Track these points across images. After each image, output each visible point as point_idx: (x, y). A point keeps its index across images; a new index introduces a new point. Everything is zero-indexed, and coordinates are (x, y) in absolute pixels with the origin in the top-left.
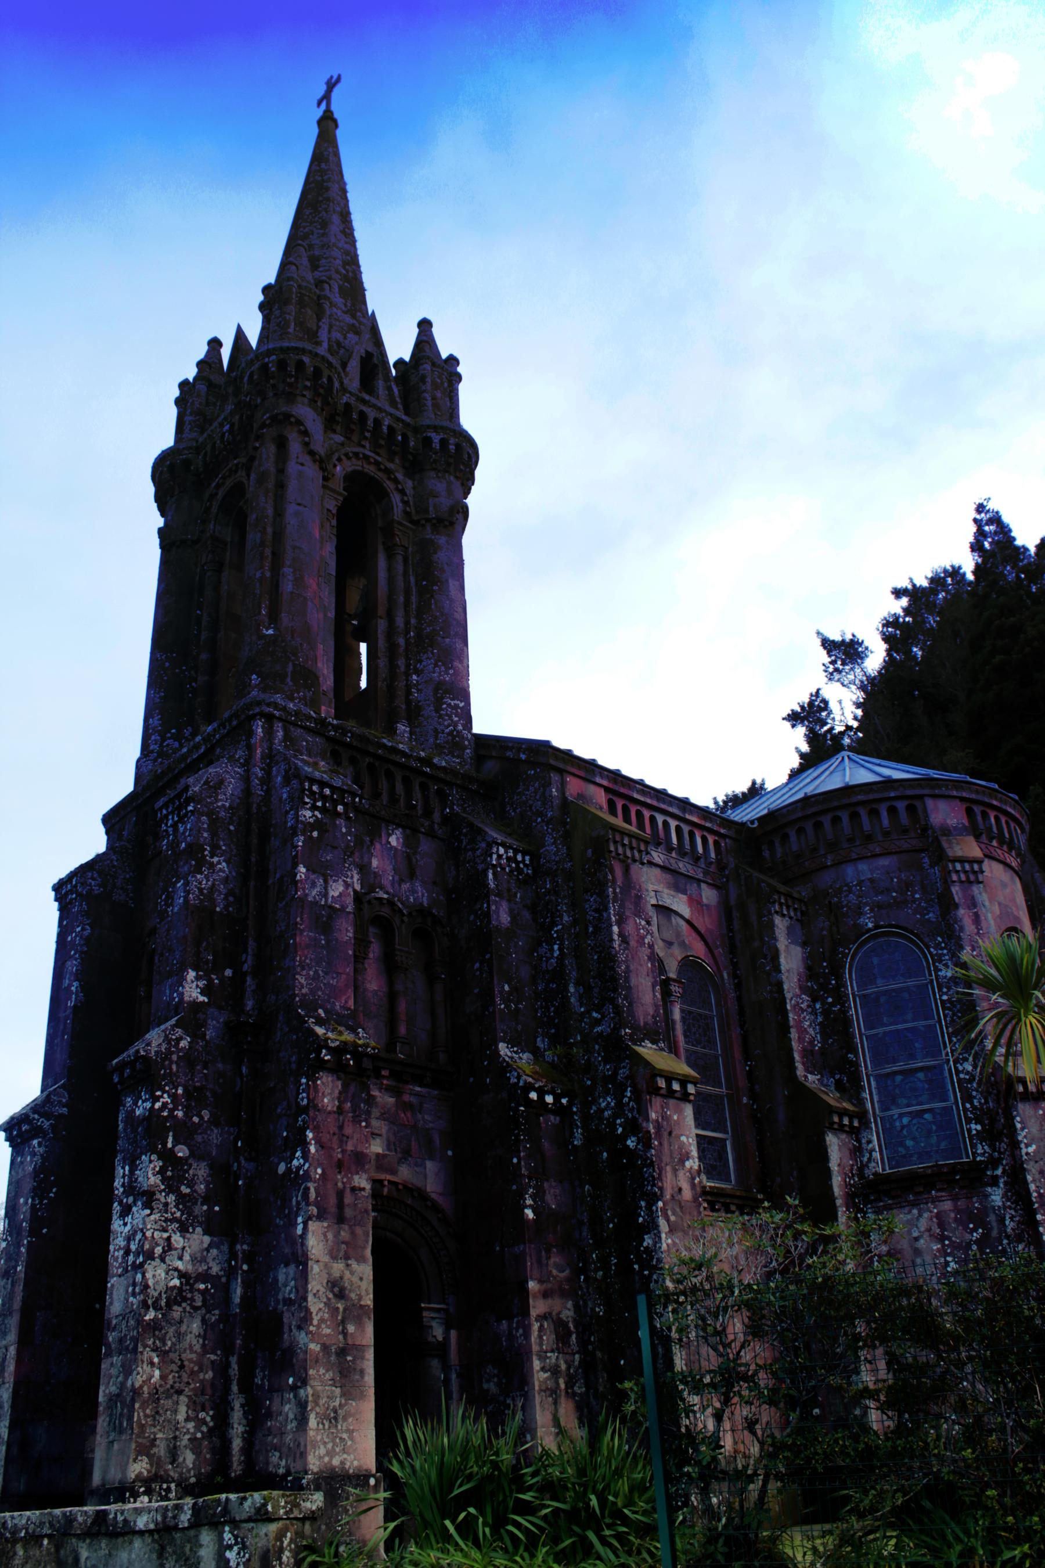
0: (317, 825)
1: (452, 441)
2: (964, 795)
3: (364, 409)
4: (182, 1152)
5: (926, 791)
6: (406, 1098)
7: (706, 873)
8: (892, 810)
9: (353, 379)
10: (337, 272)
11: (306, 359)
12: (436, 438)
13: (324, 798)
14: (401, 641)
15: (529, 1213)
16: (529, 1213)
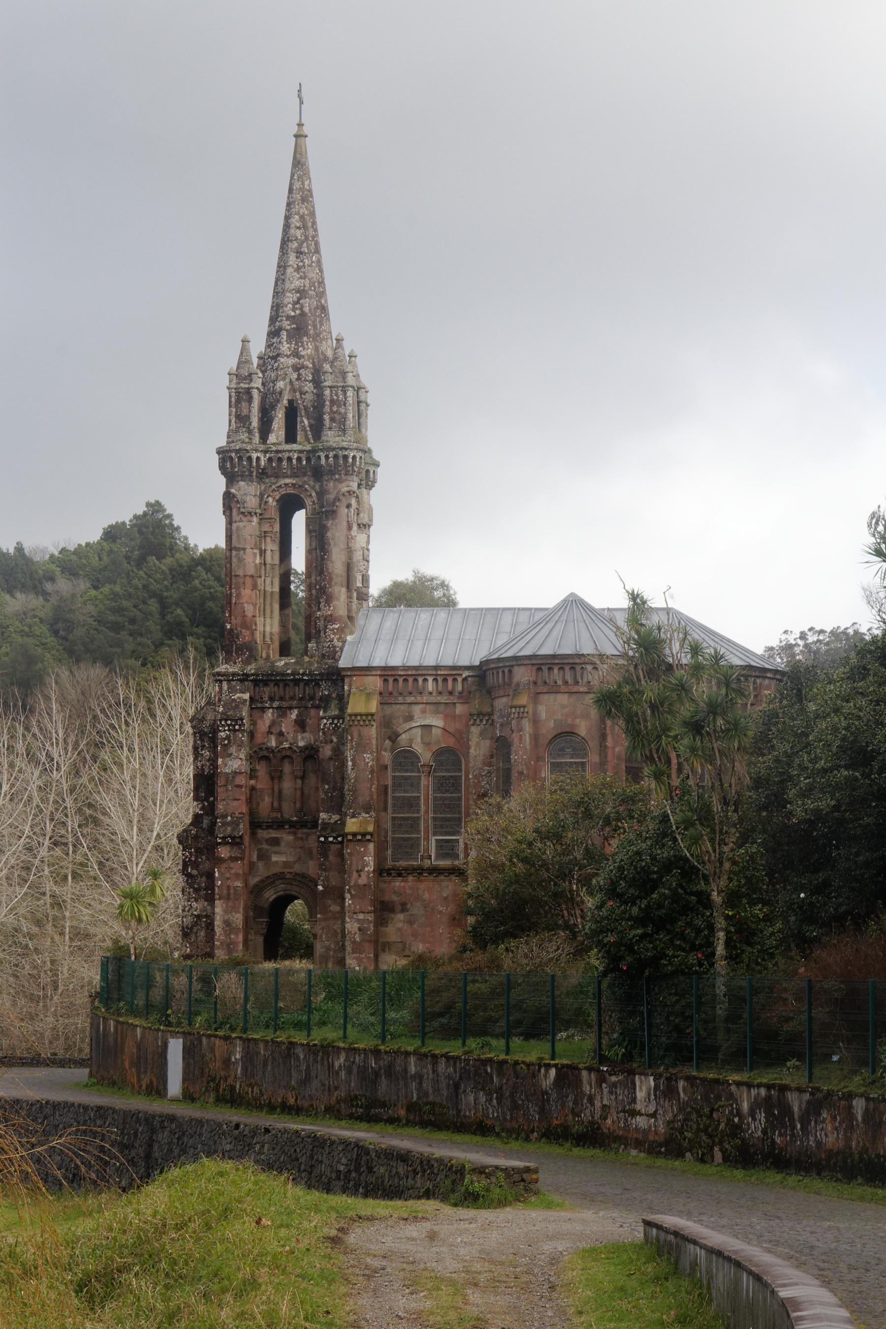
0: (228, 737)
1: (331, 454)
2: (534, 662)
3: (280, 455)
4: (195, 872)
5: (514, 663)
6: (299, 835)
7: (459, 698)
8: (503, 672)
9: (278, 434)
10: (288, 317)
11: (233, 455)
12: (322, 455)
13: (229, 726)
14: (314, 592)
15: (320, 888)
16: (320, 888)
